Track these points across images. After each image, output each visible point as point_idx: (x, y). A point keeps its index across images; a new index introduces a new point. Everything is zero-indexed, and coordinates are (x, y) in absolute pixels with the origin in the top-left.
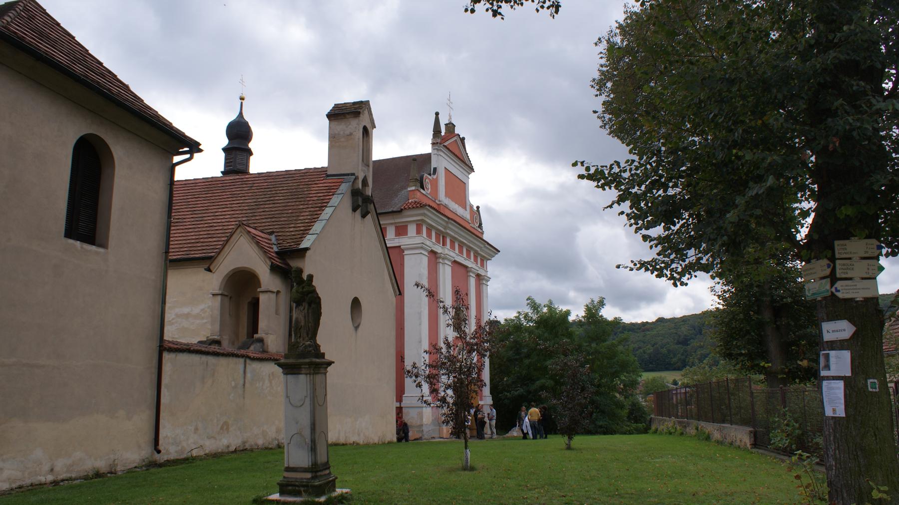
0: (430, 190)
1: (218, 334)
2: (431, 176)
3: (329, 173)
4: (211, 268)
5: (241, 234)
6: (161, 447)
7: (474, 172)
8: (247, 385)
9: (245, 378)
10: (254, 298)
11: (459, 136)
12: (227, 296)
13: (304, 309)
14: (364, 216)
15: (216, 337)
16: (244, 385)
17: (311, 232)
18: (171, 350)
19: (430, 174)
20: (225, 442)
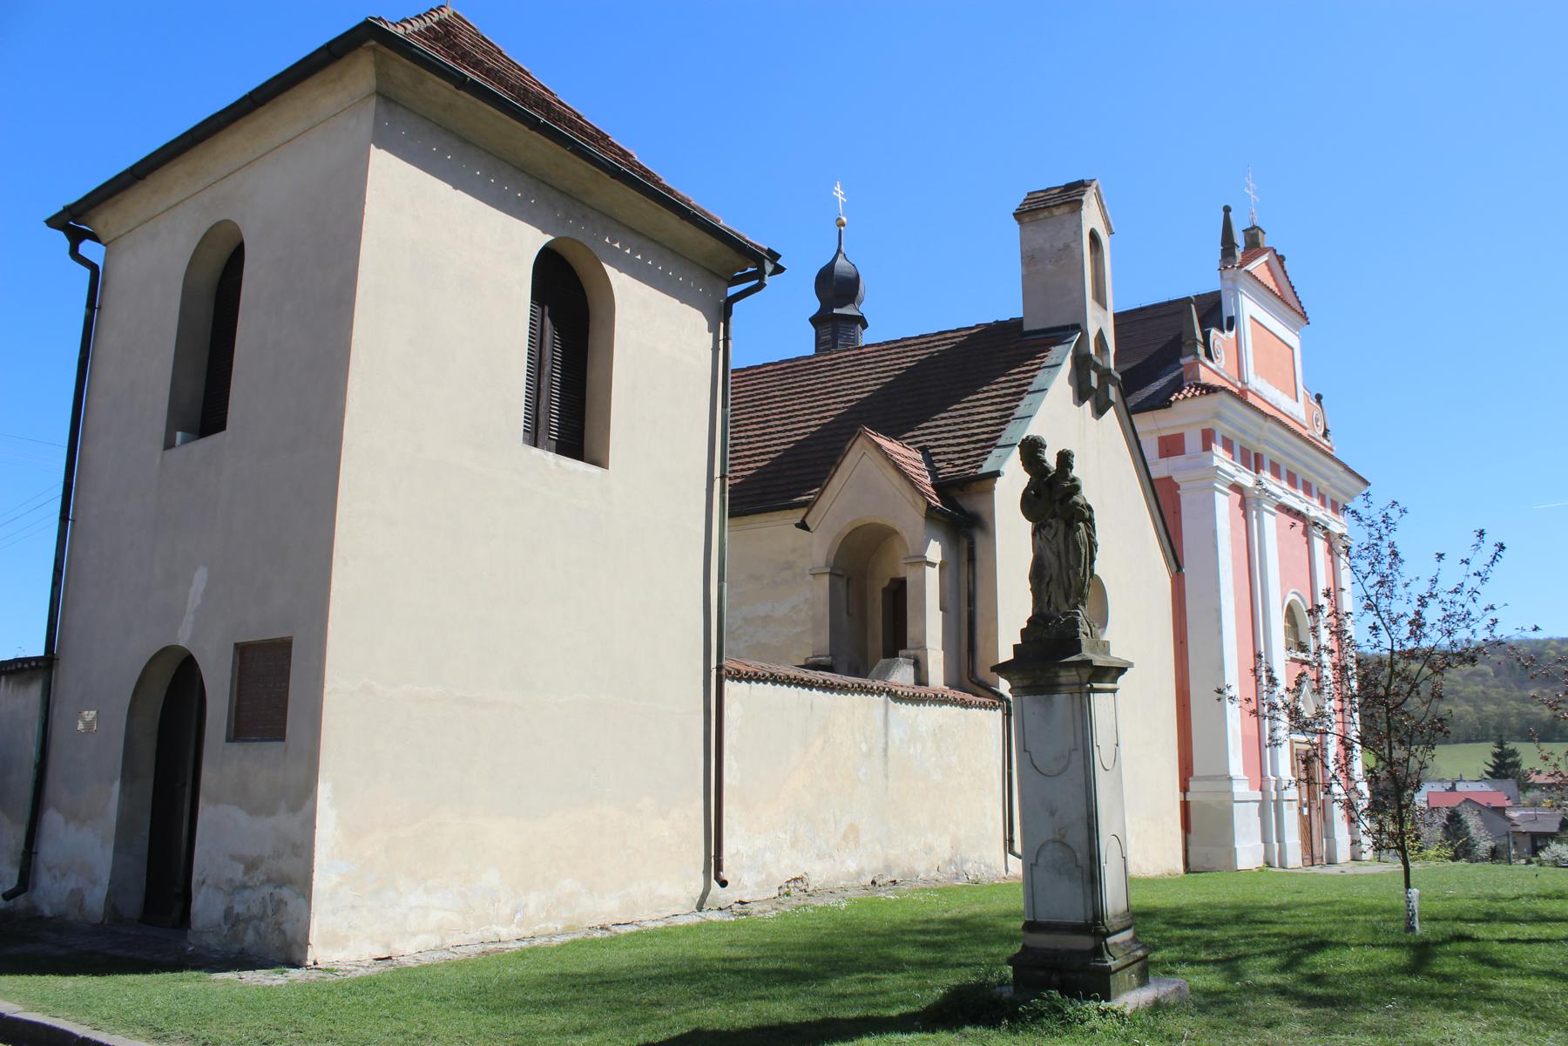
0: (1223, 362)
1: (828, 652)
3: (1026, 328)
4: (808, 521)
6: (725, 875)
8: (891, 751)
9: (886, 735)
10: (893, 580)
11: (1275, 251)
12: (841, 576)
13: (1056, 534)
14: (1099, 411)
16: (886, 750)
17: (1000, 442)
18: (739, 677)
19: (1222, 330)
20: (852, 866)
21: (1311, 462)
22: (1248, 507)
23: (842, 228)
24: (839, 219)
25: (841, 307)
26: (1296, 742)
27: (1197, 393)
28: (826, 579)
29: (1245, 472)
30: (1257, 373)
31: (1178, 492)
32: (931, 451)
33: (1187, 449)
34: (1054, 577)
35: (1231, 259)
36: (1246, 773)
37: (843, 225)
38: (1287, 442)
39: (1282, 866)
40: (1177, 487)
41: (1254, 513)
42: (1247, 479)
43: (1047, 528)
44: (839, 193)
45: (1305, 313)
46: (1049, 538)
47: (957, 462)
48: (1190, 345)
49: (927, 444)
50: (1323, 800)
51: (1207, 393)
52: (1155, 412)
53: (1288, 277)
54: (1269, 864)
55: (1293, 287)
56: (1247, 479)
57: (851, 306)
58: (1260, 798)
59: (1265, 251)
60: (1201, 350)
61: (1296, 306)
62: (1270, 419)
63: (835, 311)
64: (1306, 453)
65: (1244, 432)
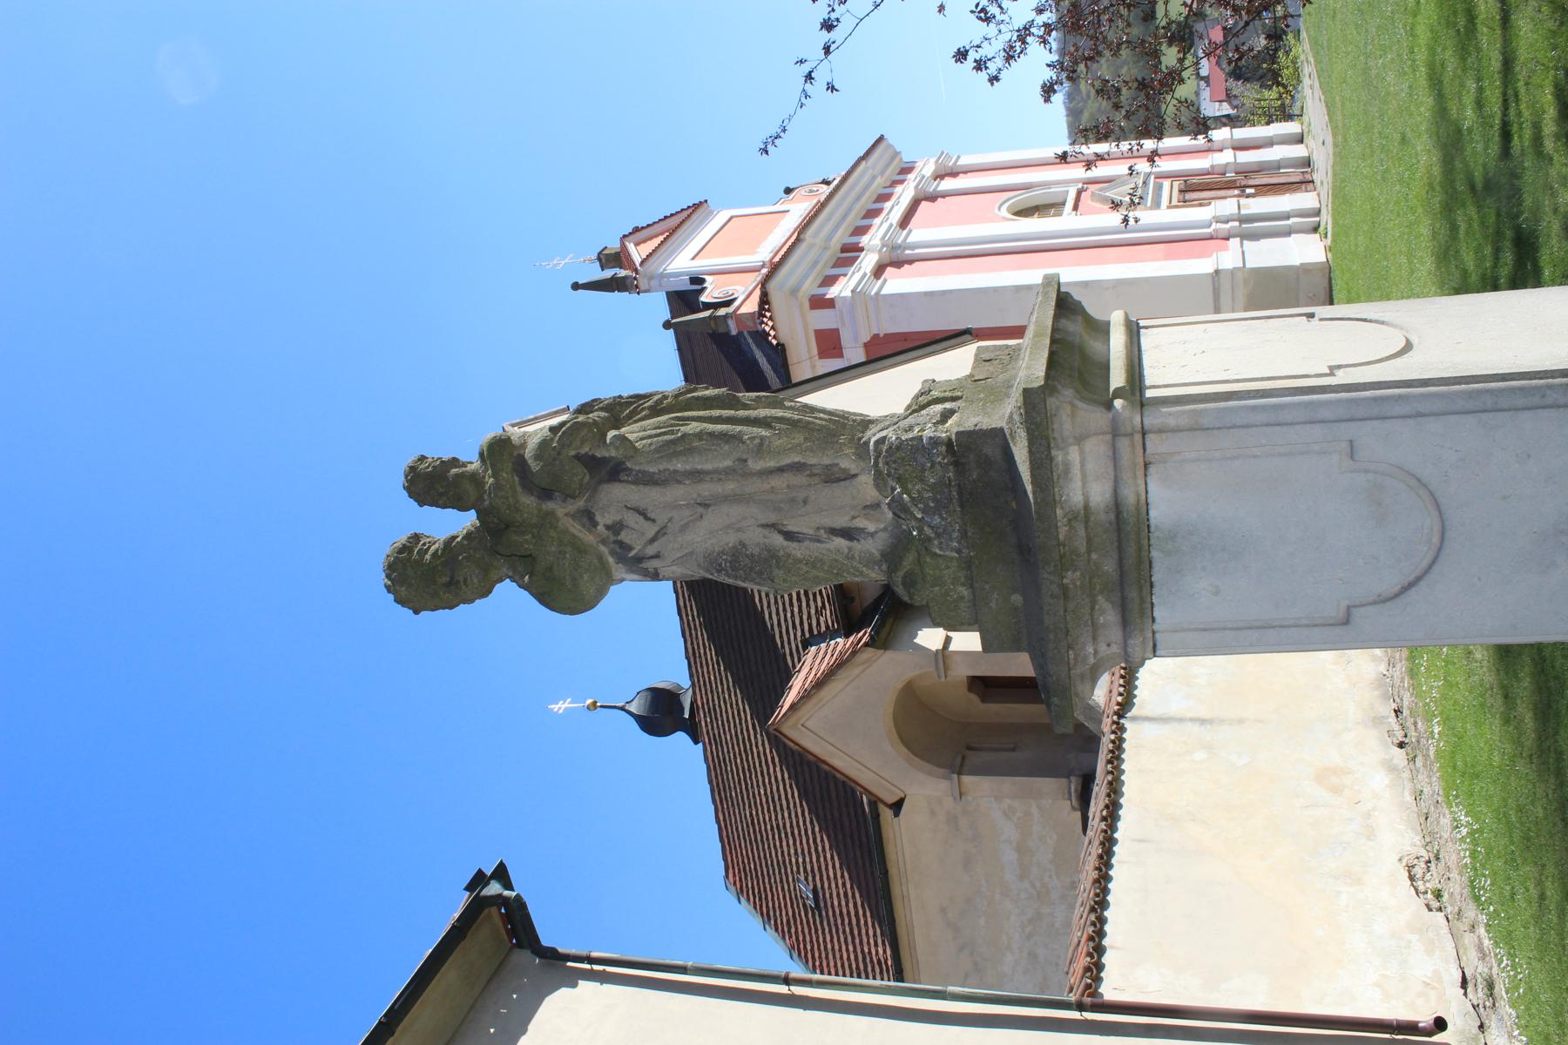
0: (737, 287)
1: (1064, 781)
4: (892, 799)
5: (800, 726)
6: (1425, 1018)
7: (706, 201)
8: (1203, 713)
9: (1181, 720)
10: (970, 689)
11: (625, 236)
12: (964, 758)
15: (1073, 787)
16: (1203, 721)
18: (1095, 970)
19: (703, 289)
20: (1379, 781)
21: (853, 194)
22: (901, 259)
23: (598, 704)
24: (588, 708)
25: (683, 709)
26: (1170, 202)
27: (768, 314)
28: (966, 779)
29: (860, 263)
30: (753, 252)
31: (881, 336)
32: (807, 635)
33: (833, 326)
34: (772, 518)
35: (628, 282)
36: (1210, 256)
37: (595, 703)
38: (828, 219)
39: (1318, 213)
40: (876, 336)
41: (908, 252)
42: (868, 261)
43: (624, 536)
44: (560, 707)
46: (651, 530)
47: (820, 604)
48: (716, 324)
49: (799, 639)
50: (1236, 173)
51: (768, 302)
52: (790, 362)
53: (654, 223)
54: (1315, 229)
55: (666, 217)
56: (868, 261)
57: (682, 698)
58: (1238, 239)
60: (722, 312)
61: (685, 214)
62: (802, 236)
63: (687, 716)
64: (843, 199)
65: (815, 263)
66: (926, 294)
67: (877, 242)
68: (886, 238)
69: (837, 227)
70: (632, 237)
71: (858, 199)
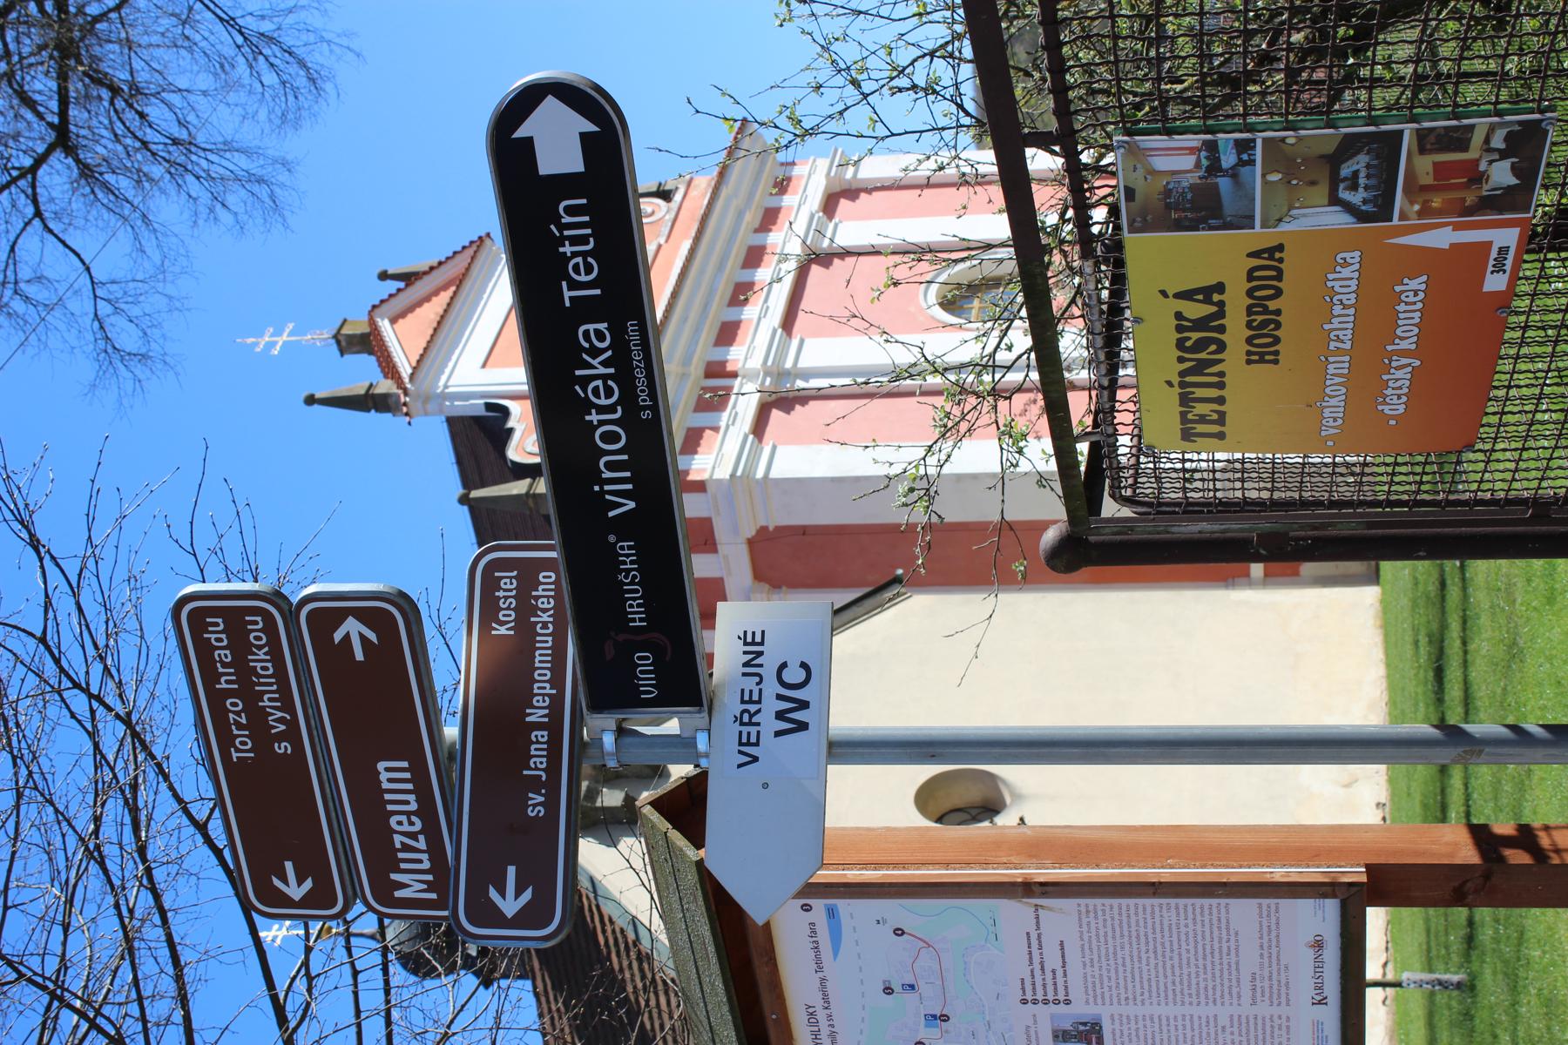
2: (511, 431)
11: (374, 307)
21: (714, 258)
29: (734, 407)
31: (771, 529)
33: (704, 514)
35: (391, 401)
38: (684, 320)
40: (763, 530)
41: (800, 384)
45: (472, 243)
48: (536, 503)
56: (745, 405)
59: (372, 322)
66: (833, 480)
67: (755, 363)
68: (769, 363)
69: (697, 331)
70: (385, 307)
71: (721, 267)
